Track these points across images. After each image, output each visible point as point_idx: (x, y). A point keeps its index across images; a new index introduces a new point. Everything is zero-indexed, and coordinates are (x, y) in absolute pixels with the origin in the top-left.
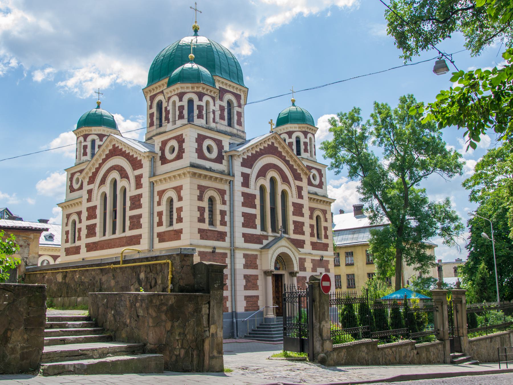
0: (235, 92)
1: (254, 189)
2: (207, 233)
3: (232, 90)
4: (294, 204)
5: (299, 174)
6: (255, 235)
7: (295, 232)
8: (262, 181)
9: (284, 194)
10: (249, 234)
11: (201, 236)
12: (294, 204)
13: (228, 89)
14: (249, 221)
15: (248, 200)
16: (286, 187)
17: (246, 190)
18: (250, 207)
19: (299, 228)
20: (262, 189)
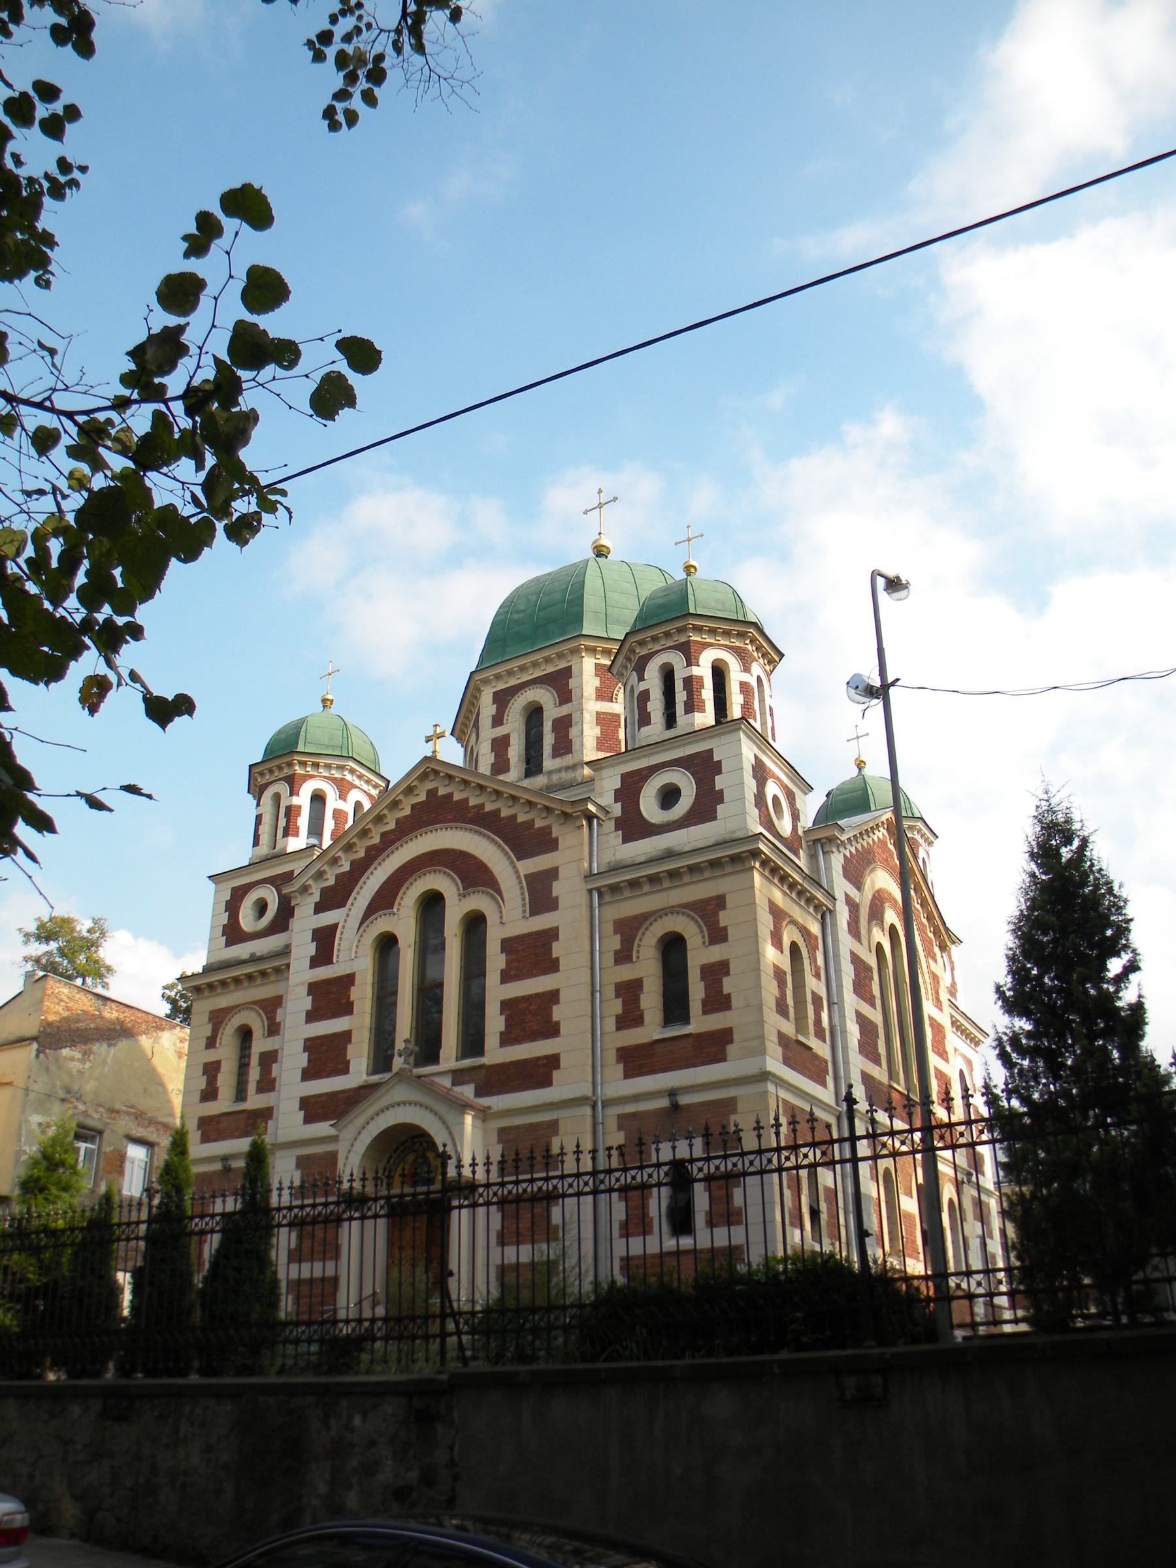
0: (538, 673)
1: (355, 957)
2: (218, 1122)
3: (526, 677)
4: (508, 945)
5: (547, 830)
6: (343, 1092)
7: (506, 1039)
8: (382, 924)
9: (475, 924)
10: (321, 1095)
11: (202, 1135)
12: (508, 945)
13: (513, 682)
14: (326, 1056)
15: (330, 998)
16: (479, 902)
17: (324, 973)
18: (334, 1015)
19: (530, 1018)
20: (387, 944)
